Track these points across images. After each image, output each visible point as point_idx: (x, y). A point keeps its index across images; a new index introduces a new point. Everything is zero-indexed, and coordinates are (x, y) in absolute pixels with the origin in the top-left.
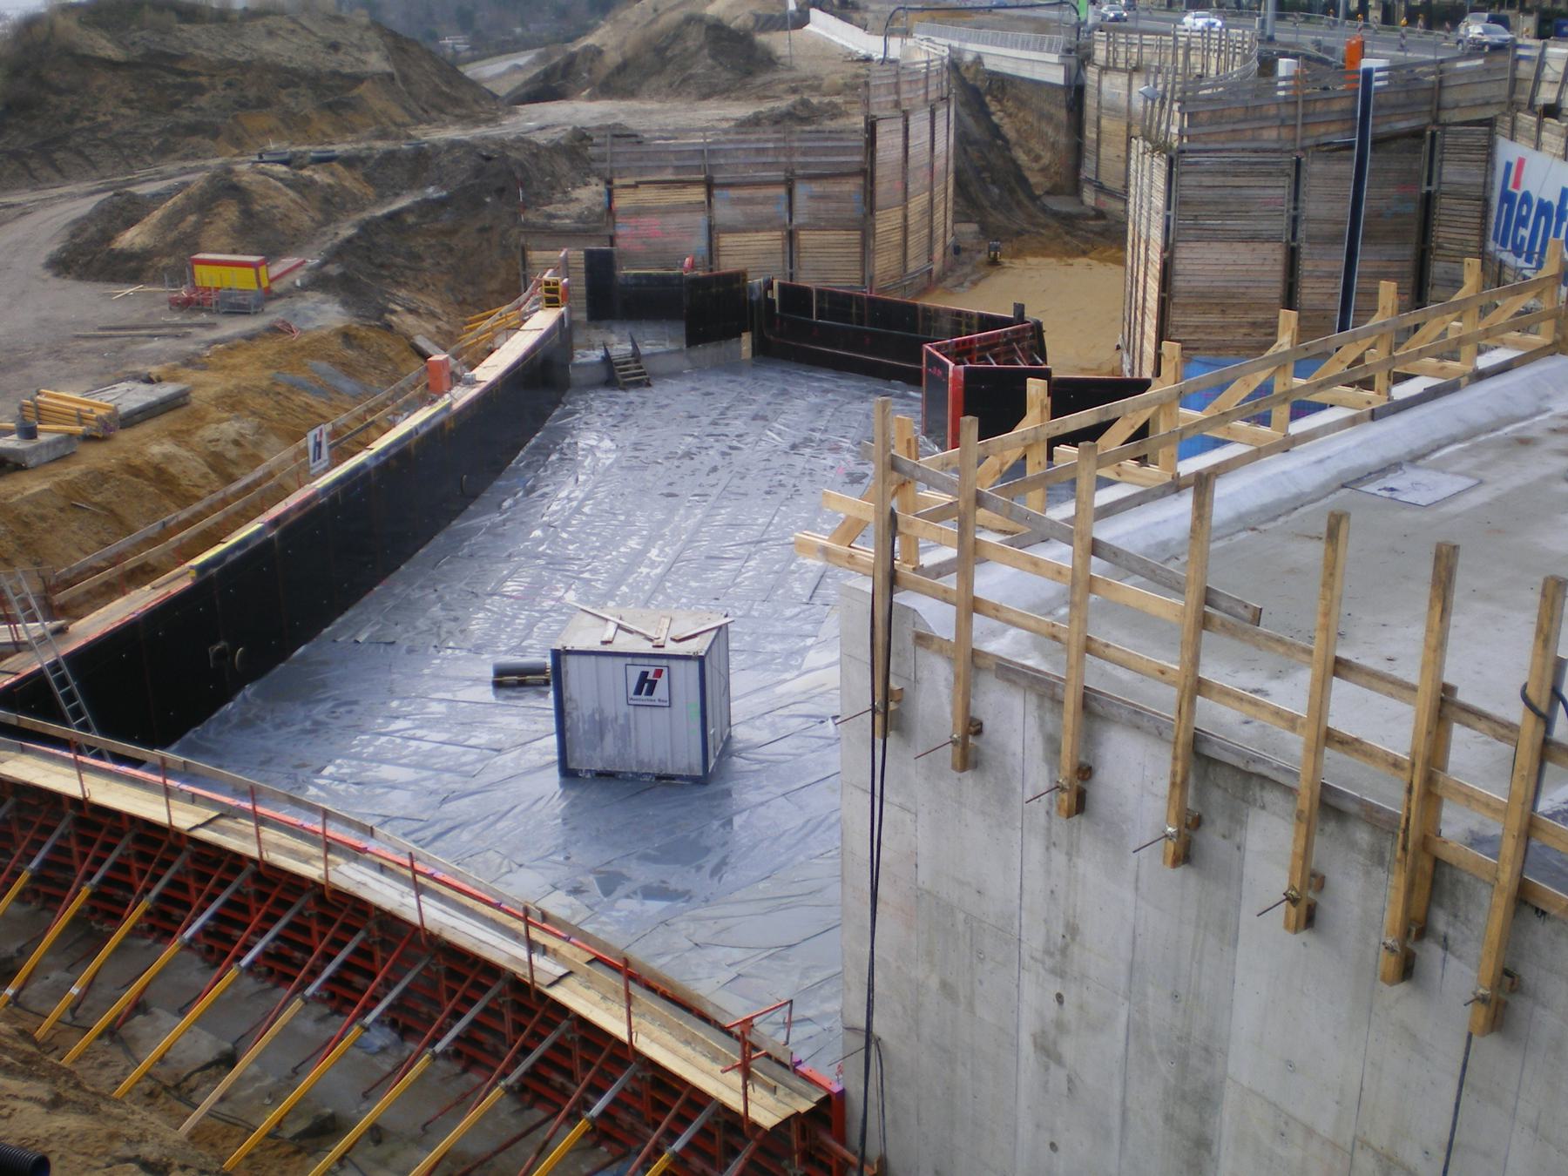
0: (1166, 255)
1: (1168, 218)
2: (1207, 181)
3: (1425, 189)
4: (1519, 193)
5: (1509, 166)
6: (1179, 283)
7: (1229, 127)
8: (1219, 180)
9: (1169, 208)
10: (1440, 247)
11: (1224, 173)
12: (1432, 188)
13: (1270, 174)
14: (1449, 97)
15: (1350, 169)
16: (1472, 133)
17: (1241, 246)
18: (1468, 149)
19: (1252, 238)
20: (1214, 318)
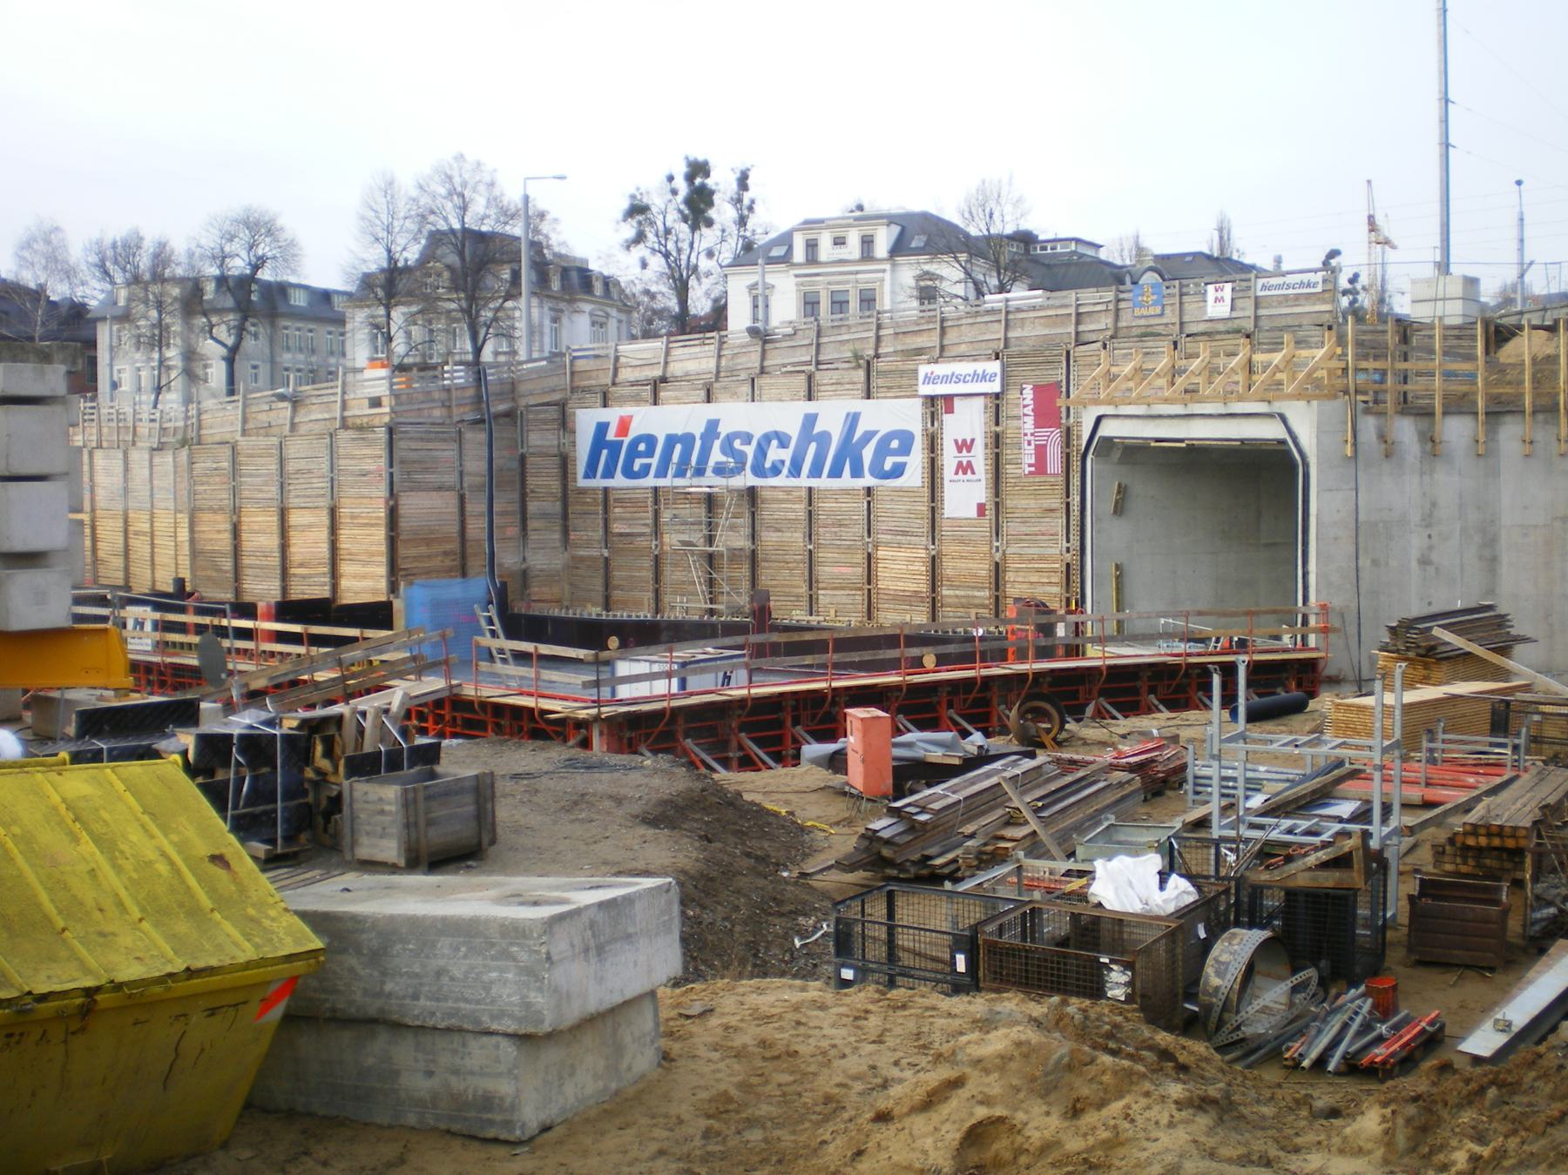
0: (391, 503)
1: (391, 475)
2: (414, 445)
3: (521, 451)
4: (627, 441)
5: (602, 428)
6: (403, 524)
7: (416, 407)
8: (420, 445)
9: (391, 466)
10: (532, 492)
11: (422, 440)
12: (525, 450)
13: (444, 440)
14: (523, 388)
15: (483, 436)
16: (546, 411)
17: (434, 494)
18: (545, 422)
19: (440, 488)
20: (423, 550)
